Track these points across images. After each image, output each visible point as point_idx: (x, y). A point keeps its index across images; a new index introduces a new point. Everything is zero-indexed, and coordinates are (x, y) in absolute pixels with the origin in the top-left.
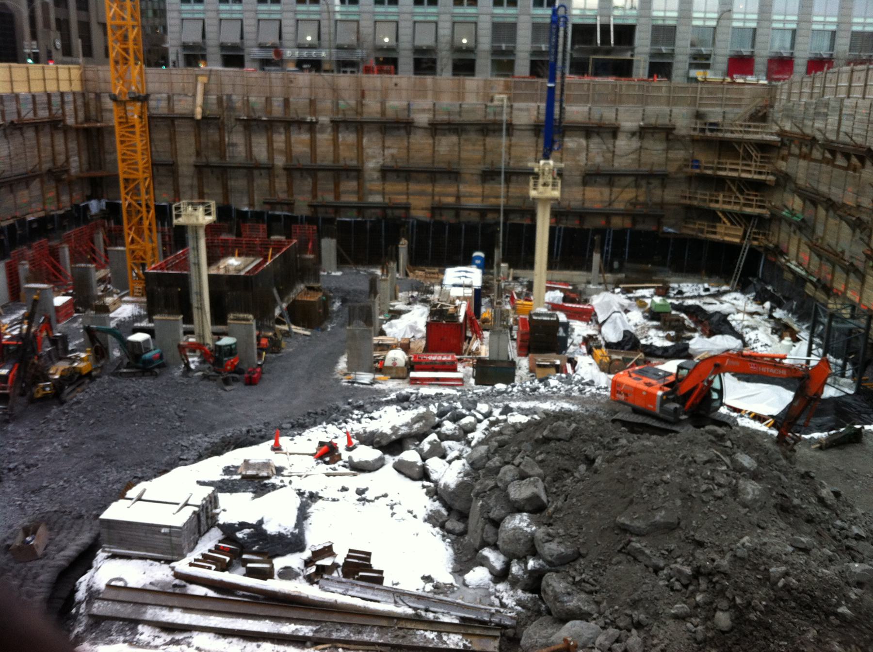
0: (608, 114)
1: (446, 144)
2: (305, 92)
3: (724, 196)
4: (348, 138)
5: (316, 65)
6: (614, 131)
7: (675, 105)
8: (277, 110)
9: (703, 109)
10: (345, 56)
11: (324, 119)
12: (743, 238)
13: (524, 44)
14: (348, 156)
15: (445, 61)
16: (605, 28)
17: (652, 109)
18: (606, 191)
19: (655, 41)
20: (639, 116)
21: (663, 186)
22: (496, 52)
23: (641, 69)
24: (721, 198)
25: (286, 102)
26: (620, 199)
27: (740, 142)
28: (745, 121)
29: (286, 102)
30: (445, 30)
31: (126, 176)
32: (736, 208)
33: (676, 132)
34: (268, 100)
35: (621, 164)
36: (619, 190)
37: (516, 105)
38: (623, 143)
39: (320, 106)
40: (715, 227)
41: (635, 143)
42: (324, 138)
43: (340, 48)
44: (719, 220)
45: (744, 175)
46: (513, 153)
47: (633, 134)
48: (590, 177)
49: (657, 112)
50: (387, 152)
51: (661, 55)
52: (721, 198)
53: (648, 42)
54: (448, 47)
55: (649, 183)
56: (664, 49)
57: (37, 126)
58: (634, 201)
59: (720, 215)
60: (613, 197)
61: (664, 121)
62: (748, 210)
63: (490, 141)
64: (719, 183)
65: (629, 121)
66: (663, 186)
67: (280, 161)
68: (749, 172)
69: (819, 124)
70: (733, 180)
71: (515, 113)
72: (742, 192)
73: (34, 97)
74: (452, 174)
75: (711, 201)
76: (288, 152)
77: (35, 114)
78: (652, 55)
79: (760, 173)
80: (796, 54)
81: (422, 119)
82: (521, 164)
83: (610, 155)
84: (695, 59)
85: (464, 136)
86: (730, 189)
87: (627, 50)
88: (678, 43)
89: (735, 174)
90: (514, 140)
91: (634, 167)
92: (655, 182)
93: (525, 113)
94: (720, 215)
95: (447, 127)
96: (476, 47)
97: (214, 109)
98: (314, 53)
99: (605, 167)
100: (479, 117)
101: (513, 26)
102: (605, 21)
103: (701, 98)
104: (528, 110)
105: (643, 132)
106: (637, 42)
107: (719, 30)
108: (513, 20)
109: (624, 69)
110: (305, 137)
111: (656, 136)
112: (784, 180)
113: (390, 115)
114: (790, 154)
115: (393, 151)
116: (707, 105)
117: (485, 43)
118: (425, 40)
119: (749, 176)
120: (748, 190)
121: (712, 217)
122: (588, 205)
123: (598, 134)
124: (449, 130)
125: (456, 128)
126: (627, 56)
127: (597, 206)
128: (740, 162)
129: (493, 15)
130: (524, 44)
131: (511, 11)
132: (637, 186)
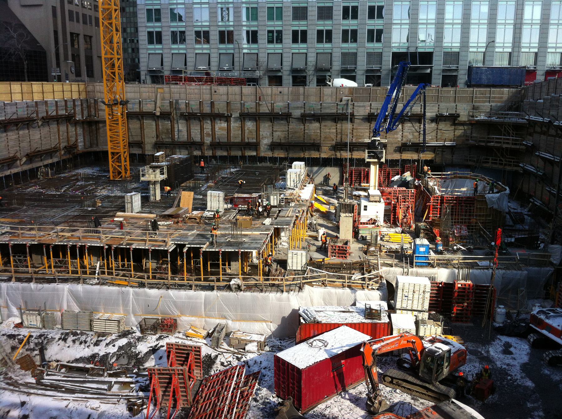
2: (225, 97)
3: (492, 159)
4: (250, 125)
7: (459, 101)
9: (476, 104)
10: (248, 75)
11: (236, 115)
13: (362, 65)
15: (311, 77)
16: (414, 55)
17: (443, 105)
23: (437, 80)
24: (490, 161)
25: (212, 104)
29: (212, 104)
31: (113, 151)
32: (501, 167)
37: (356, 104)
42: (235, 125)
45: (505, 146)
46: (355, 134)
52: (490, 161)
57: (58, 119)
67: (208, 140)
70: (498, 149)
77: (57, 112)
80: (538, 68)
81: (297, 113)
82: (360, 140)
85: (323, 124)
87: (427, 68)
89: (499, 145)
93: (363, 108)
96: (331, 68)
97: (167, 109)
102: (412, 50)
104: (364, 106)
105: (438, 119)
107: (487, 54)
108: (355, 51)
110: (224, 125)
114: (535, 132)
116: (479, 102)
118: (299, 65)
125: (319, 118)
126: (428, 71)
129: (342, 48)
130: (362, 65)
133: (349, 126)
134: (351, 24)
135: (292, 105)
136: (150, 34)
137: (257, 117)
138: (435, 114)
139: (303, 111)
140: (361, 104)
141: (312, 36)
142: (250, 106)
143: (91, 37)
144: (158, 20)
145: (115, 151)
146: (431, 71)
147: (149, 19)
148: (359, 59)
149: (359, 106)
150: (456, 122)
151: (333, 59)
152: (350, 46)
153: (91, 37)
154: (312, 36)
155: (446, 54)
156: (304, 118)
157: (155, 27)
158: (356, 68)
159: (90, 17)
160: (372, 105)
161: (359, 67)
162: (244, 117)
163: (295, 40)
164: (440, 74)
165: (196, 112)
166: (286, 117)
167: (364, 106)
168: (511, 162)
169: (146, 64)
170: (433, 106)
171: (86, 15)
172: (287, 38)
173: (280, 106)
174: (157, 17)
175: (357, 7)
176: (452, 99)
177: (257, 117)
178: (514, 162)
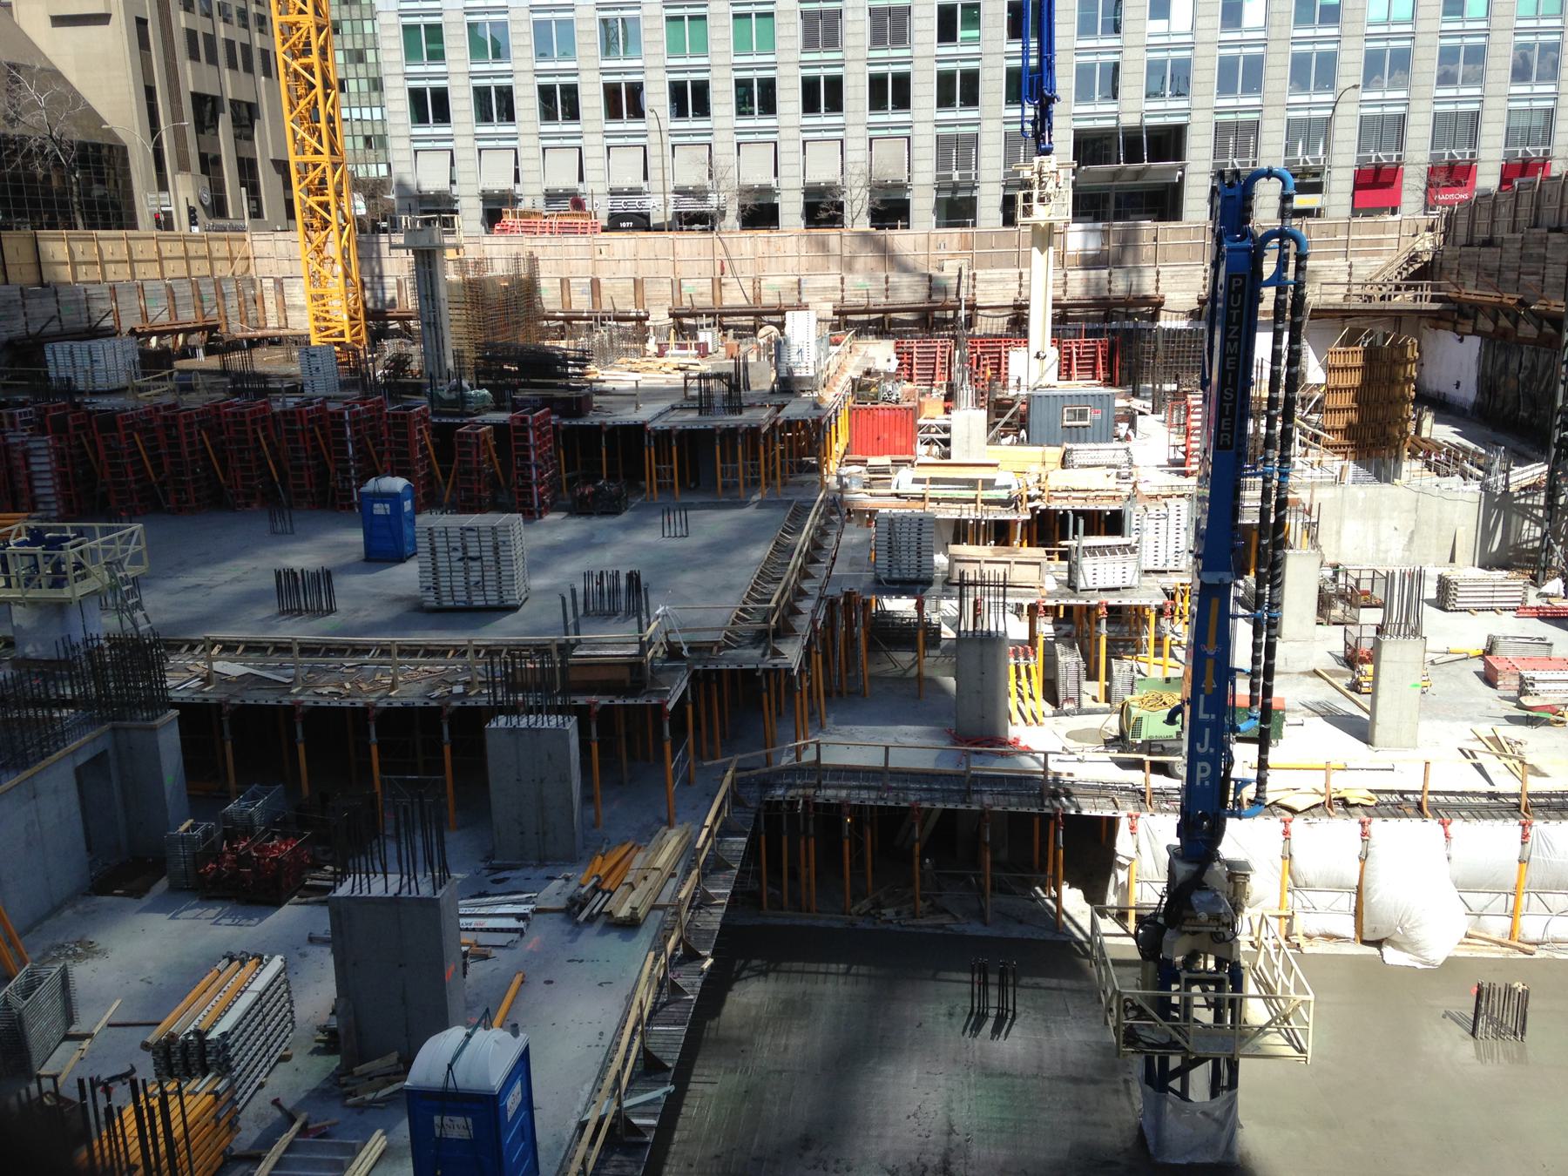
2: (627, 269)
10: (690, 205)
25: (595, 285)
29: (595, 285)
34: (565, 283)
37: (980, 274)
39: (649, 290)
43: (682, 192)
71: (980, 286)
73: (170, 288)
93: (1000, 286)
140: (995, 273)
144: (437, 55)
146: (1182, 179)
147: (412, 53)
151: (916, 153)
157: (427, 74)
171: (233, 42)
174: (433, 47)
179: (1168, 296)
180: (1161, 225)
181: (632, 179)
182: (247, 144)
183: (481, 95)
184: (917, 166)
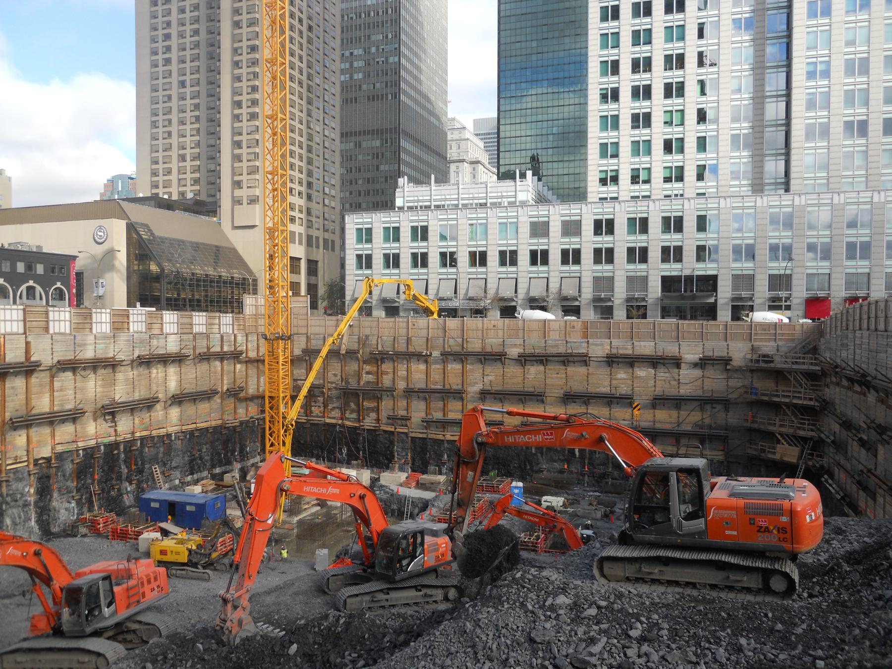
0: (671, 349)
1: (534, 371)
2: (424, 333)
3: (781, 420)
4: (454, 367)
5: (453, 313)
6: (676, 362)
7: (732, 339)
8: (401, 347)
9: (756, 344)
10: (473, 305)
11: (436, 354)
12: (800, 457)
13: (620, 292)
14: (454, 382)
17: (709, 345)
18: (674, 413)
19: (735, 287)
20: (700, 349)
21: (727, 410)
22: (597, 299)
24: (777, 422)
25: (409, 340)
26: (687, 421)
27: (790, 371)
28: (796, 353)
29: (409, 340)
30: (554, 286)
31: (270, 395)
32: (791, 431)
33: (734, 363)
35: (685, 391)
36: (687, 413)
37: (591, 341)
38: (687, 374)
40: (774, 448)
41: (698, 372)
42: (436, 368)
43: (471, 299)
44: (778, 442)
45: (795, 401)
46: (590, 381)
47: (695, 365)
48: (658, 402)
49: (717, 348)
50: (487, 379)
51: (740, 299)
52: (777, 422)
53: (730, 288)
54: (557, 296)
55: (713, 408)
56: (744, 294)
57: (221, 357)
58: (700, 423)
59: (779, 437)
60: (681, 420)
61: (720, 353)
62: (801, 433)
63: (571, 369)
64: (776, 407)
65: (691, 353)
66: (727, 410)
67: (401, 385)
68: (800, 398)
69: (844, 354)
70: (787, 405)
71: (591, 347)
72: (796, 417)
73: (222, 337)
74: (538, 397)
75: (770, 424)
76: (407, 379)
77: (222, 348)
78: (733, 300)
79: (811, 399)
80: (833, 294)
81: (514, 352)
82: (598, 390)
83: (674, 383)
84: (774, 301)
85: (548, 367)
86: (785, 414)
87: (712, 296)
88: (757, 288)
89: (787, 400)
90: (591, 370)
91: (700, 393)
92: (719, 407)
93: (600, 347)
94: (779, 437)
95: (534, 358)
96: (580, 296)
97: (355, 346)
98: (452, 305)
99: (672, 392)
100: (562, 350)
101: (645, 279)
103: (756, 334)
104: (602, 345)
105: (703, 363)
106: (720, 289)
107: (833, 276)
109: (711, 312)
110: (422, 367)
111: (716, 367)
112: (826, 406)
113: (488, 349)
114: (832, 382)
115: (491, 378)
116: (761, 340)
117: (588, 293)
119: (800, 402)
120: (802, 415)
121: (770, 437)
122: (658, 426)
123: (664, 364)
124: (537, 361)
125: (542, 359)
126: (712, 300)
127: (668, 427)
128: (792, 389)
129: (594, 271)
130: (620, 292)
131: (609, 267)
132: (702, 409)
133: (583, 370)
134: (605, 241)
135: (508, 341)
136: (359, 257)
137: (462, 357)
138: (697, 356)
139: (522, 351)
140: (598, 341)
141: (555, 257)
142: (453, 344)
143: (317, 262)
145: (273, 395)
146: (716, 300)
147: (359, 240)
148: (616, 284)
149: (596, 345)
150: (728, 367)
151: (583, 285)
152: (639, 268)
153: (317, 262)
154: (555, 257)
155: (736, 277)
156: (524, 360)
157: (365, 248)
158: (613, 296)
159: (317, 238)
160: (613, 344)
161: (616, 295)
162: (447, 356)
163: (534, 262)
164: (727, 304)
165: (386, 349)
166: (497, 357)
167: (602, 345)
168: (804, 424)
169: (351, 293)
170: (696, 346)
172: (524, 258)
173: (493, 343)
175: (681, 217)
176: (722, 336)
177: (462, 357)
178: (809, 425)
179: (733, 357)
180: (680, 322)
181: (449, 293)
182: (314, 278)
183: (387, 257)
184: (583, 290)
